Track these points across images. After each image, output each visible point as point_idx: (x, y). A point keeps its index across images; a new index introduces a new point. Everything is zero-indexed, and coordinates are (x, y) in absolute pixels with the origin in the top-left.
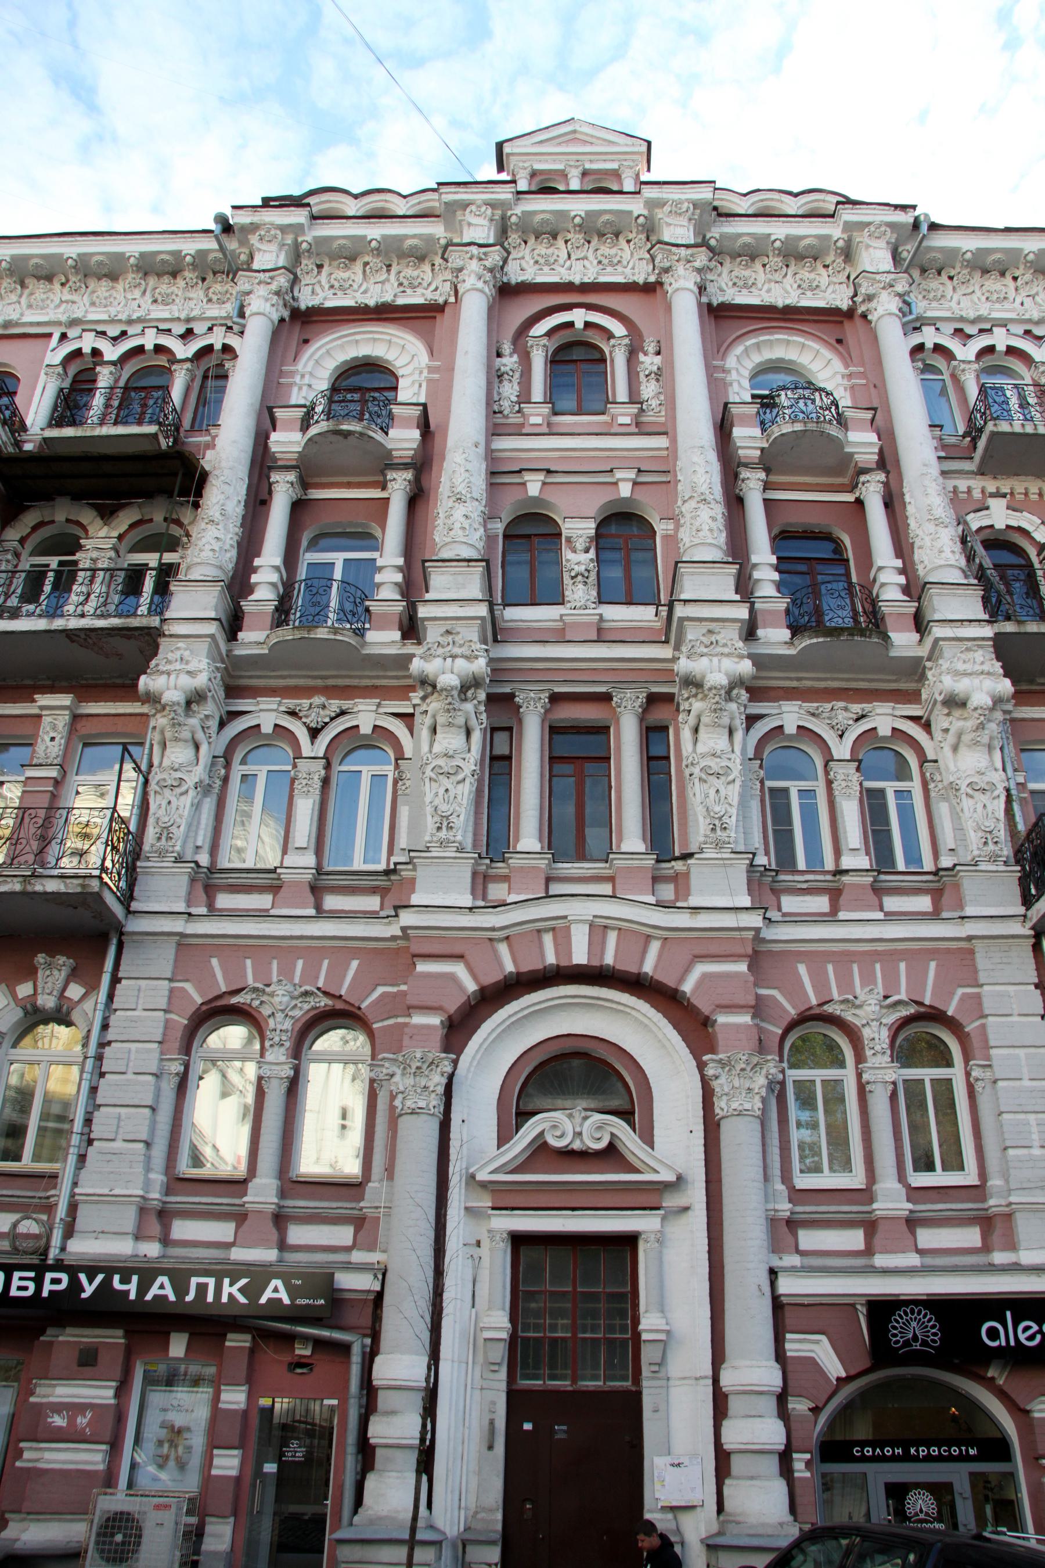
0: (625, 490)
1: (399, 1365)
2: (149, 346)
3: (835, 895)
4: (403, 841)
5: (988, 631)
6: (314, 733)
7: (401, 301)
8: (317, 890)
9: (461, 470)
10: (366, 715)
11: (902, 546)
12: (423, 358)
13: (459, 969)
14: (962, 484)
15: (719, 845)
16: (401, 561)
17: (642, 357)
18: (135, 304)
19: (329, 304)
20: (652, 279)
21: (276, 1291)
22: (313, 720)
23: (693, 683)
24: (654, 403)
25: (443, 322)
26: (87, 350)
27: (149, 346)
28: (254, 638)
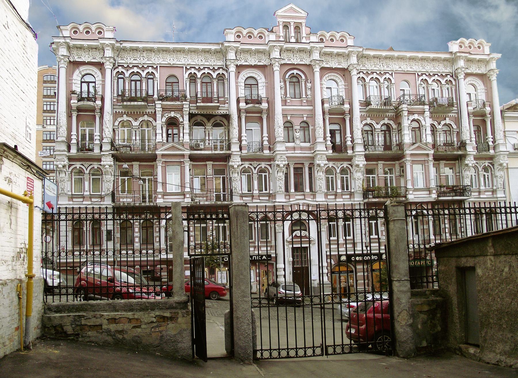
0: (305, 119)
1: (281, 265)
2: (206, 73)
3: (336, 195)
4: (271, 188)
5: (364, 153)
6: (255, 168)
7: (258, 64)
8: (259, 196)
9: (279, 120)
10: (263, 165)
11: (352, 132)
12: (263, 80)
14: (363, 114)
15: (320, 191)
16: (267, 135)
17: (307, 84)
18: (200, 59)
19: (244, 64)
21: (264, 257)
22: (255, 166)
23: (319, 165)
24: (310, 96)
25: (268, 70)
26: (193, 73)
27: (206, 73)
28: (244, 152)
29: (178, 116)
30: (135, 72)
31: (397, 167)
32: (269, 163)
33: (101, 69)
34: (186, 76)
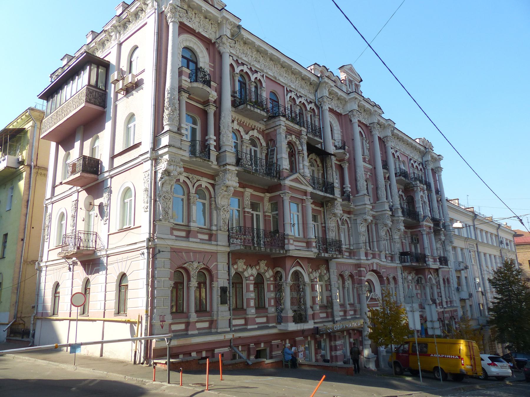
5: (403, 219)
13: (364, 269)
20: (368, 125)
29: (298, 143)
30: (245, 71)
31: (409, 235)
32: (348, 216)
33: (207, 49)
34: (288, 98)
